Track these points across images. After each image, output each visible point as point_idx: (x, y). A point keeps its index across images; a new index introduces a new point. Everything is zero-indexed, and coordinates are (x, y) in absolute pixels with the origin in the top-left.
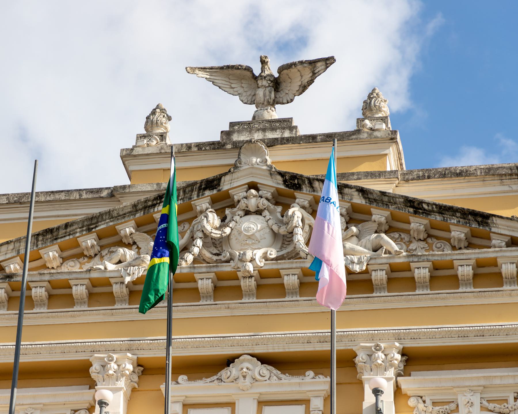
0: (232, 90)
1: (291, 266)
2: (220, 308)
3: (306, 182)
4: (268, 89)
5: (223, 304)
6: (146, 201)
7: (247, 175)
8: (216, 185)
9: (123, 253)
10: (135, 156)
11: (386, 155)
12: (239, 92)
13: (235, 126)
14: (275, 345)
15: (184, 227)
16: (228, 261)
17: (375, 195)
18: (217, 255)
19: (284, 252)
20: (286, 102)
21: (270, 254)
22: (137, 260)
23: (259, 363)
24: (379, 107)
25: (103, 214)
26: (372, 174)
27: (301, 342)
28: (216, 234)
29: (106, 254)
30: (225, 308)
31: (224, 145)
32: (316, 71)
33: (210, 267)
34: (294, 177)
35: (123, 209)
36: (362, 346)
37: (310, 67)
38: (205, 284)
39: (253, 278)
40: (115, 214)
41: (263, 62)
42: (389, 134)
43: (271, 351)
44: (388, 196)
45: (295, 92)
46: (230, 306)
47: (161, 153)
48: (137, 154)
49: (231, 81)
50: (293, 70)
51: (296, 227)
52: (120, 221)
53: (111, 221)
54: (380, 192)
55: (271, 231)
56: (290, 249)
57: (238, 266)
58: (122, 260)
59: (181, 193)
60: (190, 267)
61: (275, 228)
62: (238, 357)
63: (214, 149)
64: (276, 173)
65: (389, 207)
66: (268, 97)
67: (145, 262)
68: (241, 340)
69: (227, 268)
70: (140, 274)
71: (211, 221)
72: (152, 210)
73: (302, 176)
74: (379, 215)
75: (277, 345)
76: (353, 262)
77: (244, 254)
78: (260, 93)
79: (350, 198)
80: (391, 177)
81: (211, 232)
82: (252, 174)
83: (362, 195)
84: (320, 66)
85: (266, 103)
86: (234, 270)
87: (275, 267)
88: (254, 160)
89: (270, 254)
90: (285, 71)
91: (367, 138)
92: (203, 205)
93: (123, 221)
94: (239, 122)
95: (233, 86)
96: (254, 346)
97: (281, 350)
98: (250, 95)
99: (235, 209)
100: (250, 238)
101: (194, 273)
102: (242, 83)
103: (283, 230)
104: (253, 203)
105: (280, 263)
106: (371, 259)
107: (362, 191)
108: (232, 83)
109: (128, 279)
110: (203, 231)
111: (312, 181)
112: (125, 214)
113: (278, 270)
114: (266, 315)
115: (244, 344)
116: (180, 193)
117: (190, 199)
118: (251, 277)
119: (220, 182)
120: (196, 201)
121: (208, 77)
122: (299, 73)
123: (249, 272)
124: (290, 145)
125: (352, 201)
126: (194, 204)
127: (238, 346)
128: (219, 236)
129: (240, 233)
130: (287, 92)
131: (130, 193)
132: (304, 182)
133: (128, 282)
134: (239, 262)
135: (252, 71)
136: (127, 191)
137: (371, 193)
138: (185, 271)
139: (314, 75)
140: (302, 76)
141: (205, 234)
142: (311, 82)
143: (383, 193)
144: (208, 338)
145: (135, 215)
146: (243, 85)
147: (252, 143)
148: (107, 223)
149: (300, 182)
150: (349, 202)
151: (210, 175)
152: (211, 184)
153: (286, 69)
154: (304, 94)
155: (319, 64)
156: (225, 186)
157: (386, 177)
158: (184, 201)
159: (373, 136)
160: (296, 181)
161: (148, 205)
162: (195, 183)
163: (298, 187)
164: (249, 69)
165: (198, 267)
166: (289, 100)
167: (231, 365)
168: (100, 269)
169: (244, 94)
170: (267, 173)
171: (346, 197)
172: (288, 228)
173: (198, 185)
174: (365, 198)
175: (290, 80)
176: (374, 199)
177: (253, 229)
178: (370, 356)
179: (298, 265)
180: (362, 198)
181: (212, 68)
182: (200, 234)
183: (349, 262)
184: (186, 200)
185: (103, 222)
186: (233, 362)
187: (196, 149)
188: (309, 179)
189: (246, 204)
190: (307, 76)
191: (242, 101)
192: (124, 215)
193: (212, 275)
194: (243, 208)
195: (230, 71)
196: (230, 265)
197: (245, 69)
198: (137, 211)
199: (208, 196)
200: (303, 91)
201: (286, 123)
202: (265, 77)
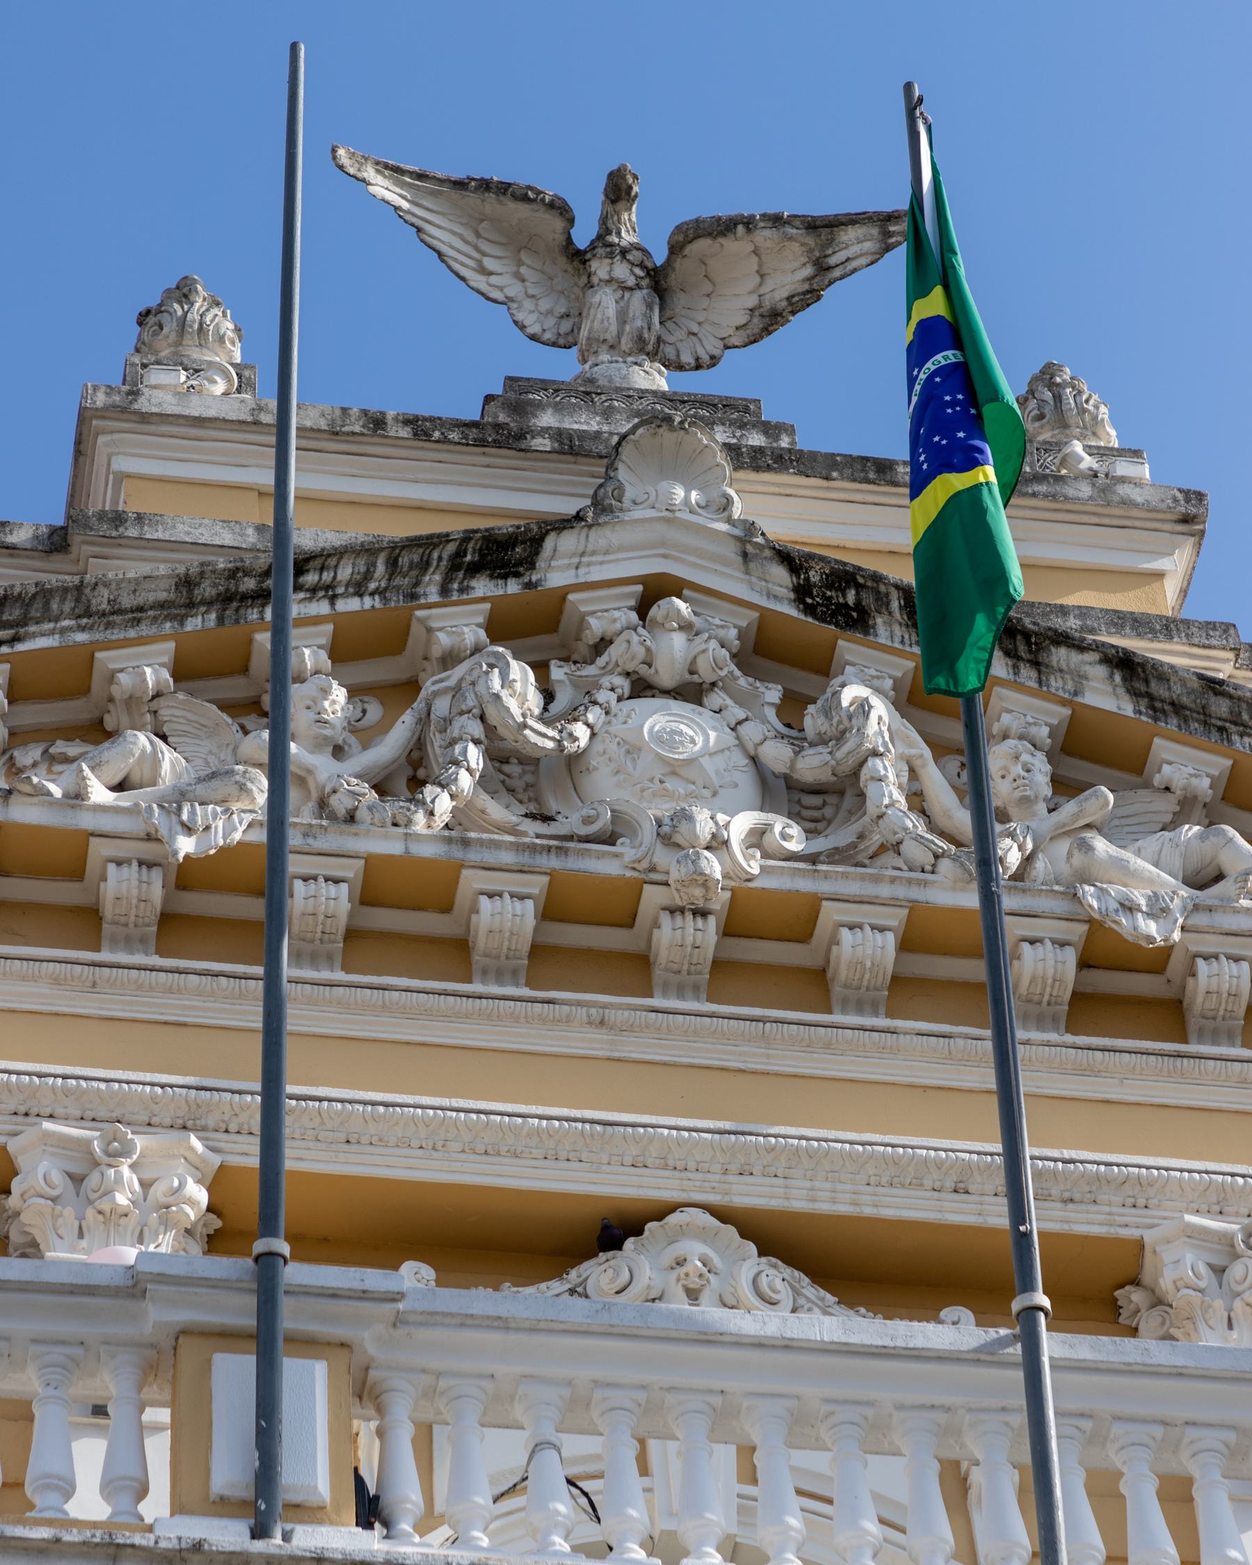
0: (483, 278)
1: (869, 890)
2: (569, 1020)
3: (895, 605)
4: (638, 294)
5: (579, 1004)
6: (233, 574)
7: (643, 548)
8: (519, 563)
9: (149, 748)
10: (145, 418)
11: (1160, 575)
12: (511, 292)
13: (519, 396)
14: (817, 1185)
15: (364, 712)
16: (610, 839)
17: (1177, 689)
18: (547, 819)
19: (821, 844)
20: (692, 362)
21: (785, 837)
22: (215, 783)
23: (752, 1248)
24: (1095, 418)
25: (51, 591)
26: (1135, 620)
27: (928, 1183)
28: (542, 738)
29: (35, 765)
30: (576, 1023)
31: (521, 435)
32: (833, 261)
33: (533, 849)
34: (844, 577)
35: (137, 585)
36: (1189, 1225)
37: (811, 241)
38: (504, 915)
39: (712, 920)
40: (101, 600)
41: (618, 190)
42: (1175, 500)
43: (799, 1205)
44: (1231, 697)
45: (731, 332)
46: (611, 1015)
47: (256, 423)
48: (155, 410)
49: (484, 246)
51: (875, 754)
52: (116, 635)
53: (82, 629)
54: (1201, 677)
55: (751, 769)
56: (840, 837)
57: (655, 860)
58: (135, 777)
59: (381, 568)
60: (449, 841)
61: (777, 754)
62: (662, 1212)
63: (481, 443)
64: (767, 553)
65: (1229, 740)
66: (639, 323)
67: (249, 792)
68: (679, 1143)
69: (604, 865)
70: (237, 836)
71: (516, 690)
72: (253, 615)
73: (877, 578)
74: (1186, 764)
75: (828, 1186)
76: (1129, 908)
77: (684, 816)
78: (605, 303)
79: (1070, 686)
80: (1214, 642)
81: (525, 726)
82: (662, 544)
83: (1124, 679)
85: (625, 344)
86: (636, 874)
87: (805, 885)
88: (679, 492)
89: (785, 837)
90: (703, 245)
91: (1091, 498)
92: (466, 629)
93: (132, 633)
94: (543, 381)
95: (489, 263)
96: (730, 1178)
97: (843, 1209)
98: (550, 312)
99: (590, 670)
100: (674, 773)
101: (462, 865)
102: (520, 263)
103: (813, 765)
104: (673, 652)
105: (826, 876)
106: (1196, 908)
108: (484, 254)
109: (186, 845)
110: (482, 718)
112: (140, 609)
113: (813, 905)
114: (754, 1073)
115: (692, 1165)
116: (374, 565)
117: (414, 597)
118: (701, 913)
119: (537, 553)
120: (434, 611)
121: (405, 205)
122: (756, 259)
123: (706, 882)
124: (788, 479)
125: (1079, 699)
126: (421, 621)
127: (665, 1167)
128: (550, 745)
129: (633, 750)
130: (695, 328)
131: (144, 543)
132: (883, 602)
133: (187, 857)
134: (659, 845)
135: (571, 221)
136: (132, 532)
138: (428, 851)
140: (762, 276)
141: (490, 730)
142: (808, 297)
143: (1213, 686)
144: (541, 1117)
145: (182, 620)
146: (523, 270)
147: (672, 428)
148: (63, 631)
149: (868, 600)
150: (1063, 703)
152: (503, 551)
153: (710, 235)
154: (767, 341)
155: (849, 234)
156: (558, 568)
157: (1196, 641)
158: (385, 600)
159: (1116, 499)
160: (851, 597)
161: (242, 588)
162: (444, 538)
163: (857, 621)
164: (561, 208)
165: (481, 842)
166: (705, 358)
167: (630, 1243)
168: (49, 794)
169: (528, 305)
170: (730, 551)
171: (1055, 683)
172: (840, 754)
173: (451, 548)
174: (1134, 694)
175: (707, 287)
176: (1173, 704)
177: (693, 742)
178: (1219, 1271)
179: (901, 892)
180: (1121, 691)
181: (421, 176)
182: (477, 729)
183: (1113, 905)
184: (396, 601)
185: (48, 626)
186: (638, 1232)
187: (405, 432)
189: (648, 650)
190: (790, 274)
191: (522, 327)
193: (537, 885)
194: (630, 667)
195: (491, 204)
196: (616, 855)
197: (551, 206)
198: (191, 605)
199: (483, 600)
200: (767, 331)
202: (624, 252)
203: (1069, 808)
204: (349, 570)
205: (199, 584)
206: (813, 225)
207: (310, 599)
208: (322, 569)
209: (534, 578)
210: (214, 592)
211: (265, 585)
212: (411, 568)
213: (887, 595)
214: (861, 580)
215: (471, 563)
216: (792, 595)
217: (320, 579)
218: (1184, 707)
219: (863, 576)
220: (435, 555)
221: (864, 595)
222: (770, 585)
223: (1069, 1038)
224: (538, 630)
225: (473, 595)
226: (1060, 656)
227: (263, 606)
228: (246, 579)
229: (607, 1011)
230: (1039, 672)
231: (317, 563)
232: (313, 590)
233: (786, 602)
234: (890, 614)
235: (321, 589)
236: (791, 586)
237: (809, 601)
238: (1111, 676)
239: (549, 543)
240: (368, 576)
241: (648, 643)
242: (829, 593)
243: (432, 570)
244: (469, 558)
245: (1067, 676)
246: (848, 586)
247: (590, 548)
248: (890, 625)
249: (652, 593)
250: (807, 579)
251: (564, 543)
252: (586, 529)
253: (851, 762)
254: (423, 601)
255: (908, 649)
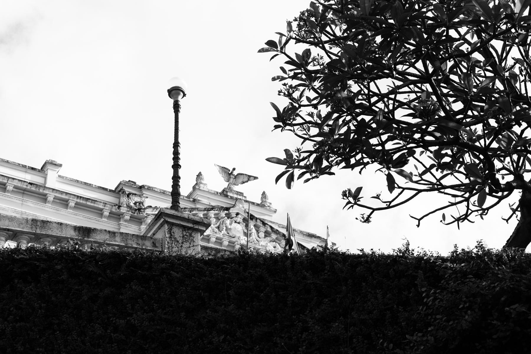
28: (229, 227)
41: (234, 169)
50: (242, 176)
61: (246, 231)
69: (233, 240)
71: (228, 222)
74: (274, 236)
78: (232, 180)
84: (252, 178)
107: (271, 227)
139: (249, 180)
142: (247, 182)
143: (277, 230)
151: (228, 206)
152: (227, 209)
156: (231, 211)
163: (252, 219)
164: (229, 170)
190: (246, 179)
192: (201, 211)
201: (241, 194)
206: (249, 176)
224: (229, 216)
249: (237, 214)
251: (232, 209)
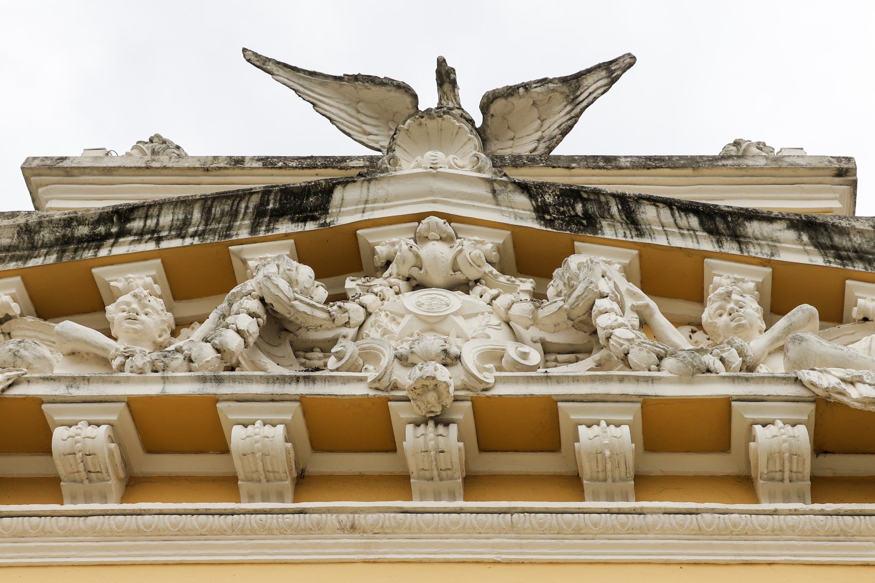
2: (319, 528)
3: (614, 210)
5: (329, 511)
34: (572, 194)
59: (197, 215)
64: (511, 187)
72: (89, 254)
73: (597, 193)
83: (811, 238)
111: (633, 205)
119: (328, 202)
137: (843, 232)
149: (593, 208)
150: (764, 263)
160: (579, 208)
162: (250, 193)
170: (484, 191)
173: (255, 200)
174: (821, 248)
176: (856, 251)
188: (622, 199)
198: (33, 248)
199: (286, 236)
203: (782, 323)
204: (170, 218)
205: (39, 232)
207: (139, 241)
208: (146, 218)
209: (328, 221)
210: (52, 238)
211: (97, 231)
212: (223, 214)
213: (607, 203)
214: (585, 196)
215: (273, 210)
216: (534, 215)
217: (145, 225)
218: (868, 253)
219: (586, 192)
220: (243, 205)
221: (589, 206)
222: (516, 211)
223: (817, 507)
225: (276, 232)
226: (753, 228)
227: (99, 247)
228: (80, 227)
229: (356, 516)
230: (739, 243)
231: (142, 212)
232: (141, 234)
233: (530, 220)
234: (612, 217)
235: (148, 233)
236: (532, 208)
237: (548, 217)
238: (800, 236)
239: (337, 194)
240: (186, 223)
241: (414, 248)
242: (562, 209)
243: (241, 216)
244: (271, 206)
245: (762, 242)
246: (576, 202)
247: (371, 197)
248: (614, 226)
250: (544, 201)
252: (366, 183)
253: (583, 306)
254: (234, 238)
255: (630, 240)
